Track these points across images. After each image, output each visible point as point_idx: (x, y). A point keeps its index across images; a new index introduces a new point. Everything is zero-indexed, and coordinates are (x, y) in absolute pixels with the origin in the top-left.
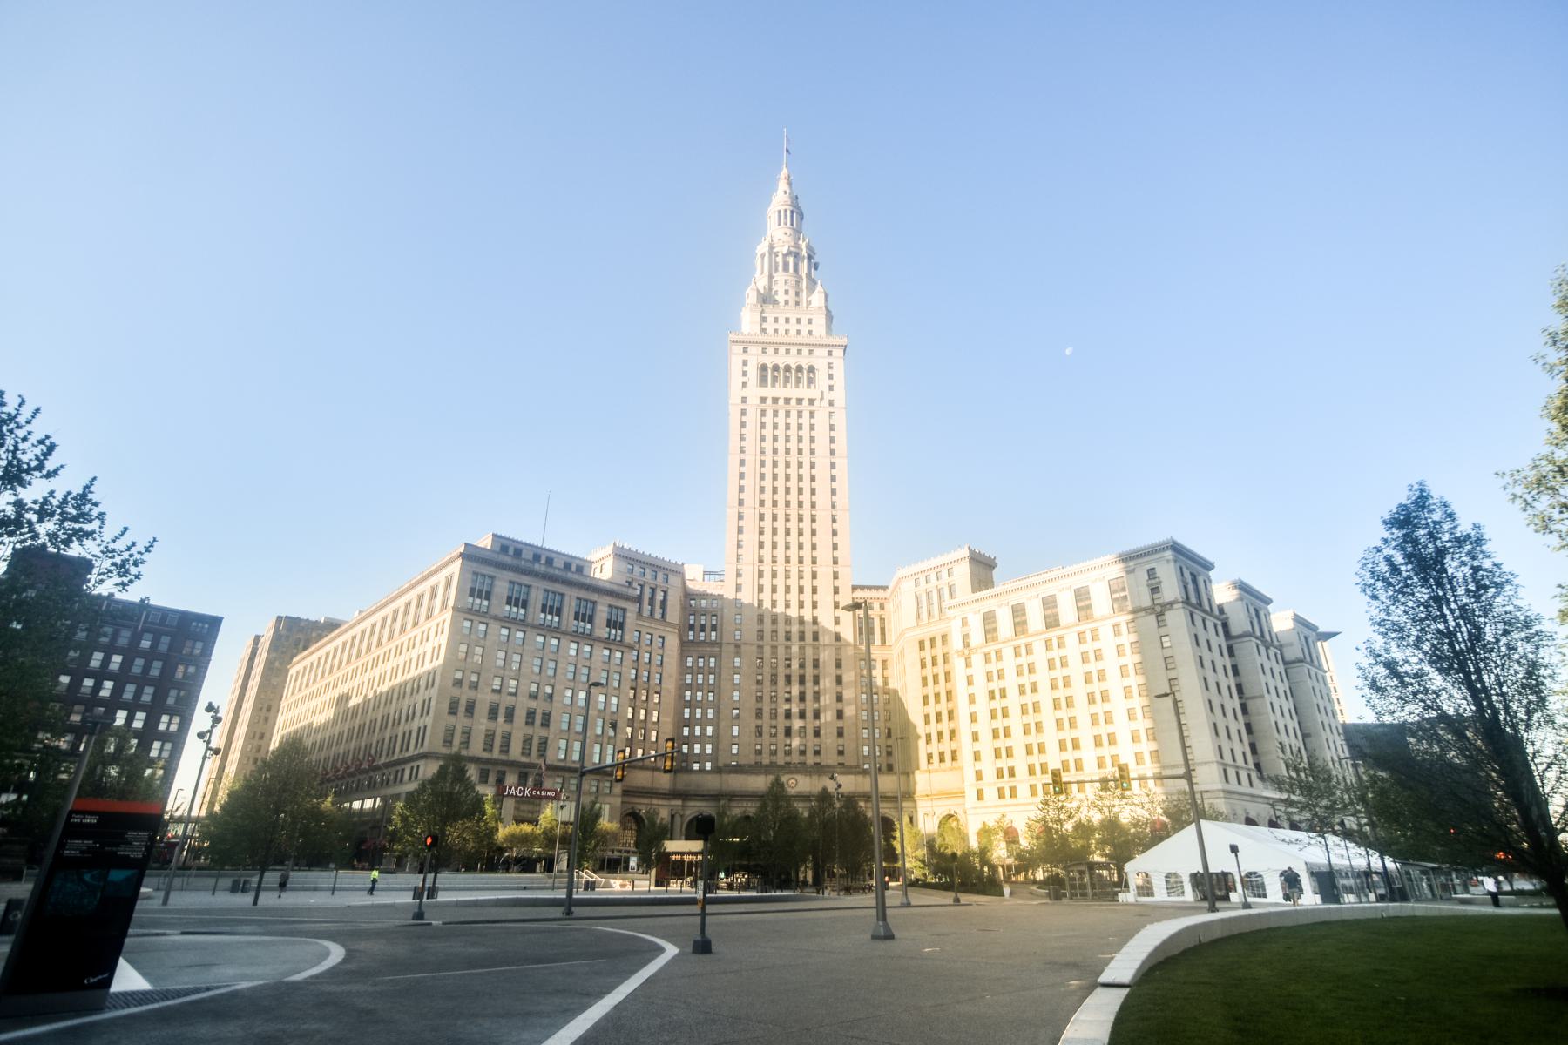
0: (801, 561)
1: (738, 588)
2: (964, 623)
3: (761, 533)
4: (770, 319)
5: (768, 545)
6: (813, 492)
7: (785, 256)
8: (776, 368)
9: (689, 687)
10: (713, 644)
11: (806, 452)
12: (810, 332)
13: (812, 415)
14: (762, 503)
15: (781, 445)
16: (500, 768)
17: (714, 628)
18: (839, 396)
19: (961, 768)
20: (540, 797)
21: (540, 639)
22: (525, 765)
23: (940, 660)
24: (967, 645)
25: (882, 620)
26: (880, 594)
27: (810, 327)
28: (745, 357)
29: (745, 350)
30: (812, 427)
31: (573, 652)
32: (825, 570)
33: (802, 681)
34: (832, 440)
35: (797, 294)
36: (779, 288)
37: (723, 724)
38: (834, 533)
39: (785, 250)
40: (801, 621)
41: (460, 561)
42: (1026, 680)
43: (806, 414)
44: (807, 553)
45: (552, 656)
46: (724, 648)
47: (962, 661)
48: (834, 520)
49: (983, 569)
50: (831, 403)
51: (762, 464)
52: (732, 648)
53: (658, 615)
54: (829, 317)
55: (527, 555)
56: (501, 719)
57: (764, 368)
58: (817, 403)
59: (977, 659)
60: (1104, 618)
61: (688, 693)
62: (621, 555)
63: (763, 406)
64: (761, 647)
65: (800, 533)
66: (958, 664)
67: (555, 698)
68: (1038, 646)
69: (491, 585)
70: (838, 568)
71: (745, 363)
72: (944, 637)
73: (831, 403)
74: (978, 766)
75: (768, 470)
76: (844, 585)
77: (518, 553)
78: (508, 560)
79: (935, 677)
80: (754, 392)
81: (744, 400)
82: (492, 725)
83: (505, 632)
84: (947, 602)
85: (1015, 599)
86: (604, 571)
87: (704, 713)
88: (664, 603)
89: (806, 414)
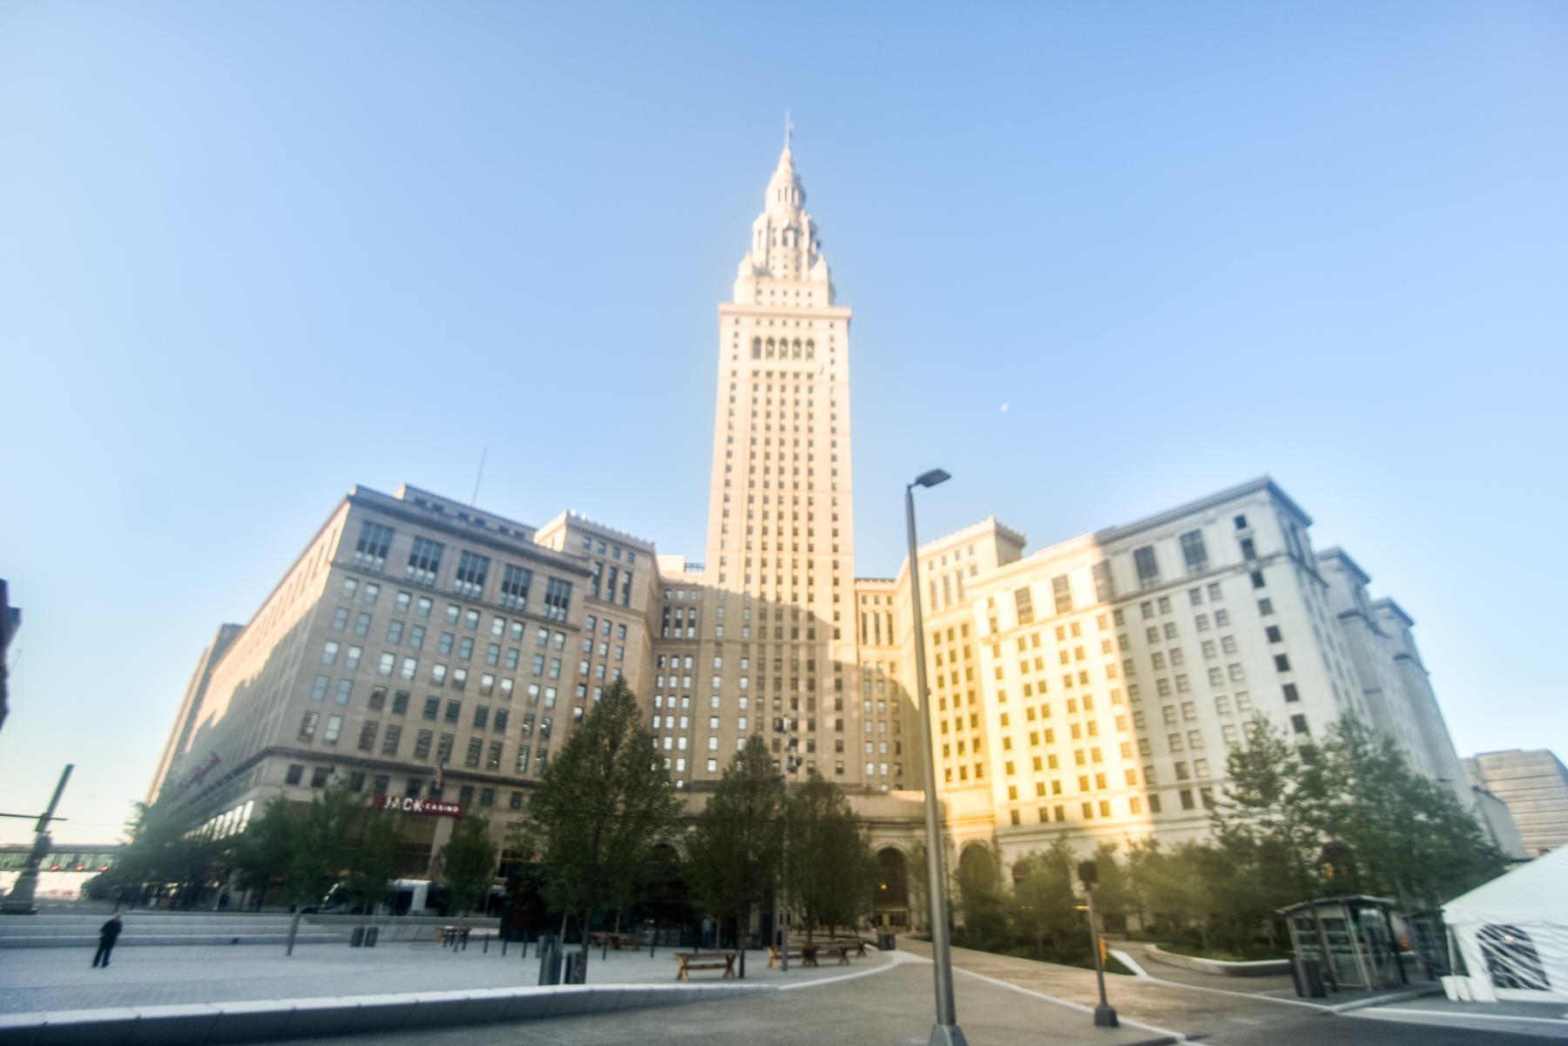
0: (795, 549)
1: (722, 578)
2: (991, 603)
3: (750, 516)
5: (757, 531)
7: (784, 231)
8: (771, 341)
9: (659, 691)
10: (689, 641)
13: (811, 390)
14: (752, 484)
16: (380, 772)
17: (692, 624)
18: (842, 370)
19: (989, 786)
20: (437, 814)
21: (453, 611)
22: (418, 770)
23: (960, 655)
24: (994, 630)
25: (890, 617)
26: (887, 586)
28: (736, 329)
31: (497, 631)
32: (823, 559)
33: (794, 683)
35: (797, 269)
37: (698, 736)
38: (835, 518)
39: (785, 224)
40: (795, 613)
41: (347, 507)
42: (1073, 668)
44: (802, 540)
45: (467, 634)
46: (703, 646)
47: (989, 650)
48: (834, 504)
49: (1011, 544)
50: (832, 378)
52: (712, 646)
53: (619, 600)
54: (832, 290)
56: (388, 709)
57: (757, 341)
58: (816, 378)
59: (1008, 647)
61: (659, 699)
62: (574, 526)
63: (756, 380)
64: (746, 645)
65: (795, 517)
66: (983, 655)
67: (468, 686)
69: (389, 540)
70: (837, 557)
72: (965, 629)
73: (832, 378)
74: (1012, 781)
76: (847, 574)
79: (955, 676)
80: (746, 364)
82: (374, 716)
83: (404, 598)
84: (967, 580)
85: (1056, 571)
86: (552, 537)
87: (677, 723)
88: (627, 588)
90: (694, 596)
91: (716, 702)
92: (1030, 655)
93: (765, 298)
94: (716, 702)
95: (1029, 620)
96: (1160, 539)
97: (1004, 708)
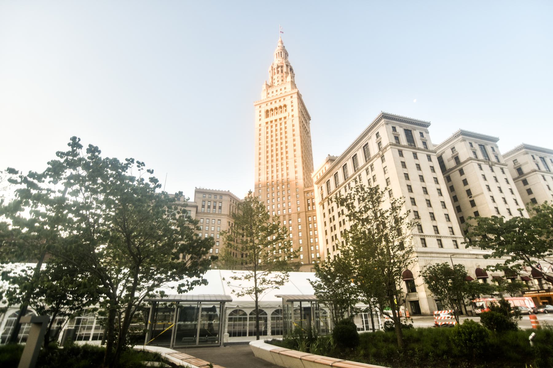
4: (271, 93)
7: (277, 68)
11: (284, 137)
13: (285, 123)
15: (274, 138)
27: (285, 90)
30: (286, 128)
43: (283, 124)
48: (295, 162)
50: (293, 116)
57: (267, 111)
58: (287, 118)
62: (198, 192)
63: (267, 125)
71: (260, 112)
73: (293, 116)
75: (269, 149)
80: (264, 120)
81: (260, 125)
89: (283, 124)
93: (270, 95)
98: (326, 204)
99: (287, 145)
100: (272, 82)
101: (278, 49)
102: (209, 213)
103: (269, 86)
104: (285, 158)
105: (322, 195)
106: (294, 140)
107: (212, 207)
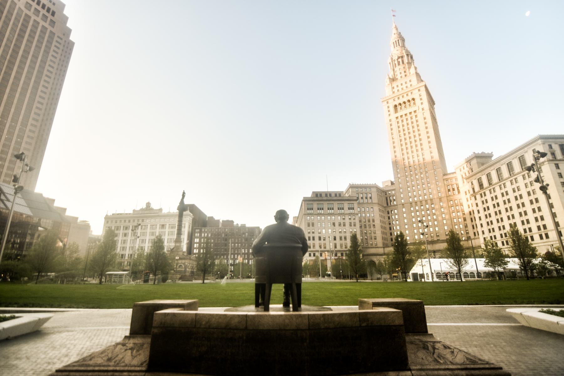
4: (395, 87)
6: (421, 145)
11: (416, 130)
12: (411, 85)
13: (416, 116)
15: (406, 132)
17: (394, 200)
24: (474, 192)
27: (411, 83)
29: (387, 103)
34: (426, 123)
35: (405, 72)
36: (398, 73)
42: (495, 202)
46: (399, 206)
50: (423, 109)
51: (401, 141)
55: (324, 195)
57: (396, 106)
59: (478, 196)
60: (518, 173)
63: (398, 120)
68: (497, 188)
71: (388, 107)
73: (423, 109)
75: (403, 142)
77: (321, 195)
78: (316, 198)
80: (393, 116)
81: (390, 121)
83: (319, 217)
90: (393, 192)
91: (406, 221)
92: (484, 199)
93: (395, 90)
94: (406, 221)
95: (483, 188)
96: (513, 159)
97: (480, 215)
98: (478, 196)
99: (420, 137)
100: (394, 75)
101: (394, 37)
102: (363, 203)
103: (393, 80)
104: (420, 150)
105: (473, 189)
106: (427, 133)
107: (364, 198)
